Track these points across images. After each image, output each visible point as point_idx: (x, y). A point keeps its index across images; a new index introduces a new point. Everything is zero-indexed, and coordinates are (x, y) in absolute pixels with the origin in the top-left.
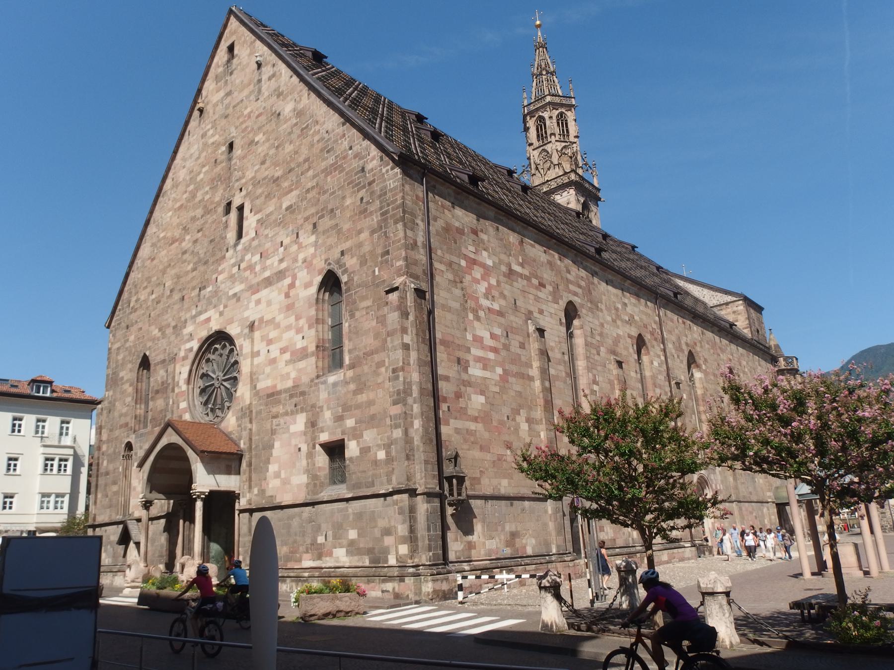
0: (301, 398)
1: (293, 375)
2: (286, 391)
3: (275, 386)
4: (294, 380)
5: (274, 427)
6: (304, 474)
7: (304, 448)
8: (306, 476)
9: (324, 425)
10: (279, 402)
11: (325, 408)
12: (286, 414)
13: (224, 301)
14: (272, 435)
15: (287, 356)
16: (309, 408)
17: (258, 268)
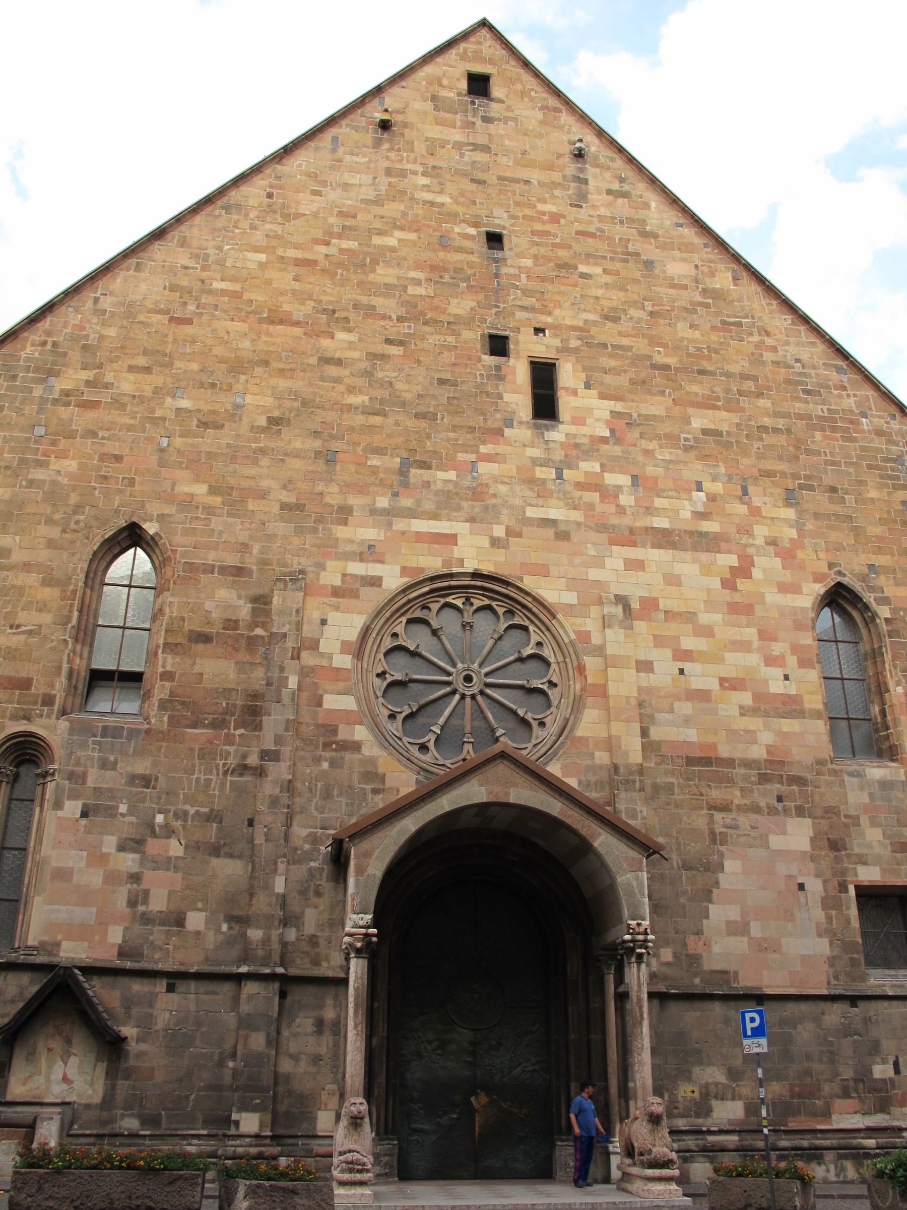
0: (795, 788)
1: (766, 738)
2: (747, 764)
3: (714, 747)
4: (769, 749)
5: (718, 829)
6: (820, 936)
7: (815, 886)
8: (825, 941)
9: (865, 851)
10: (730, 781)
11: (864, 820)
12: (755, 809)
13: (505, 516)
14: (714, 841)
15: (746, 698)
16: (818, 812)
17: (626, 500)
